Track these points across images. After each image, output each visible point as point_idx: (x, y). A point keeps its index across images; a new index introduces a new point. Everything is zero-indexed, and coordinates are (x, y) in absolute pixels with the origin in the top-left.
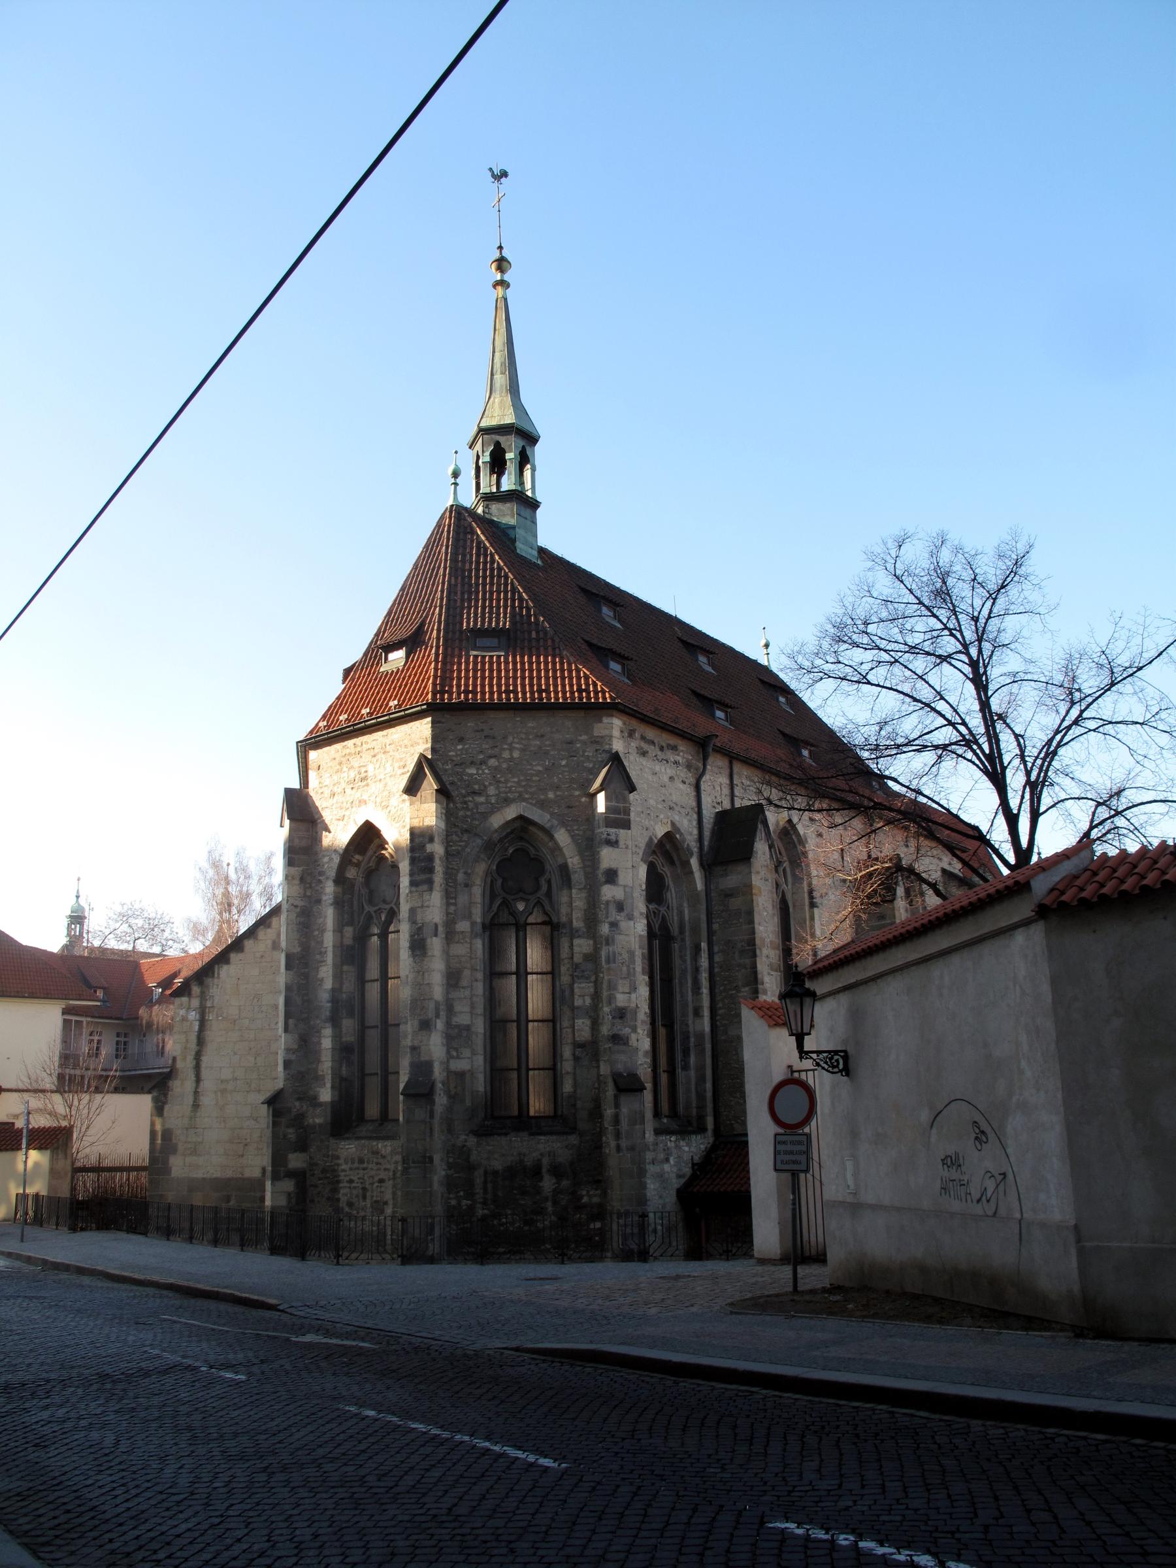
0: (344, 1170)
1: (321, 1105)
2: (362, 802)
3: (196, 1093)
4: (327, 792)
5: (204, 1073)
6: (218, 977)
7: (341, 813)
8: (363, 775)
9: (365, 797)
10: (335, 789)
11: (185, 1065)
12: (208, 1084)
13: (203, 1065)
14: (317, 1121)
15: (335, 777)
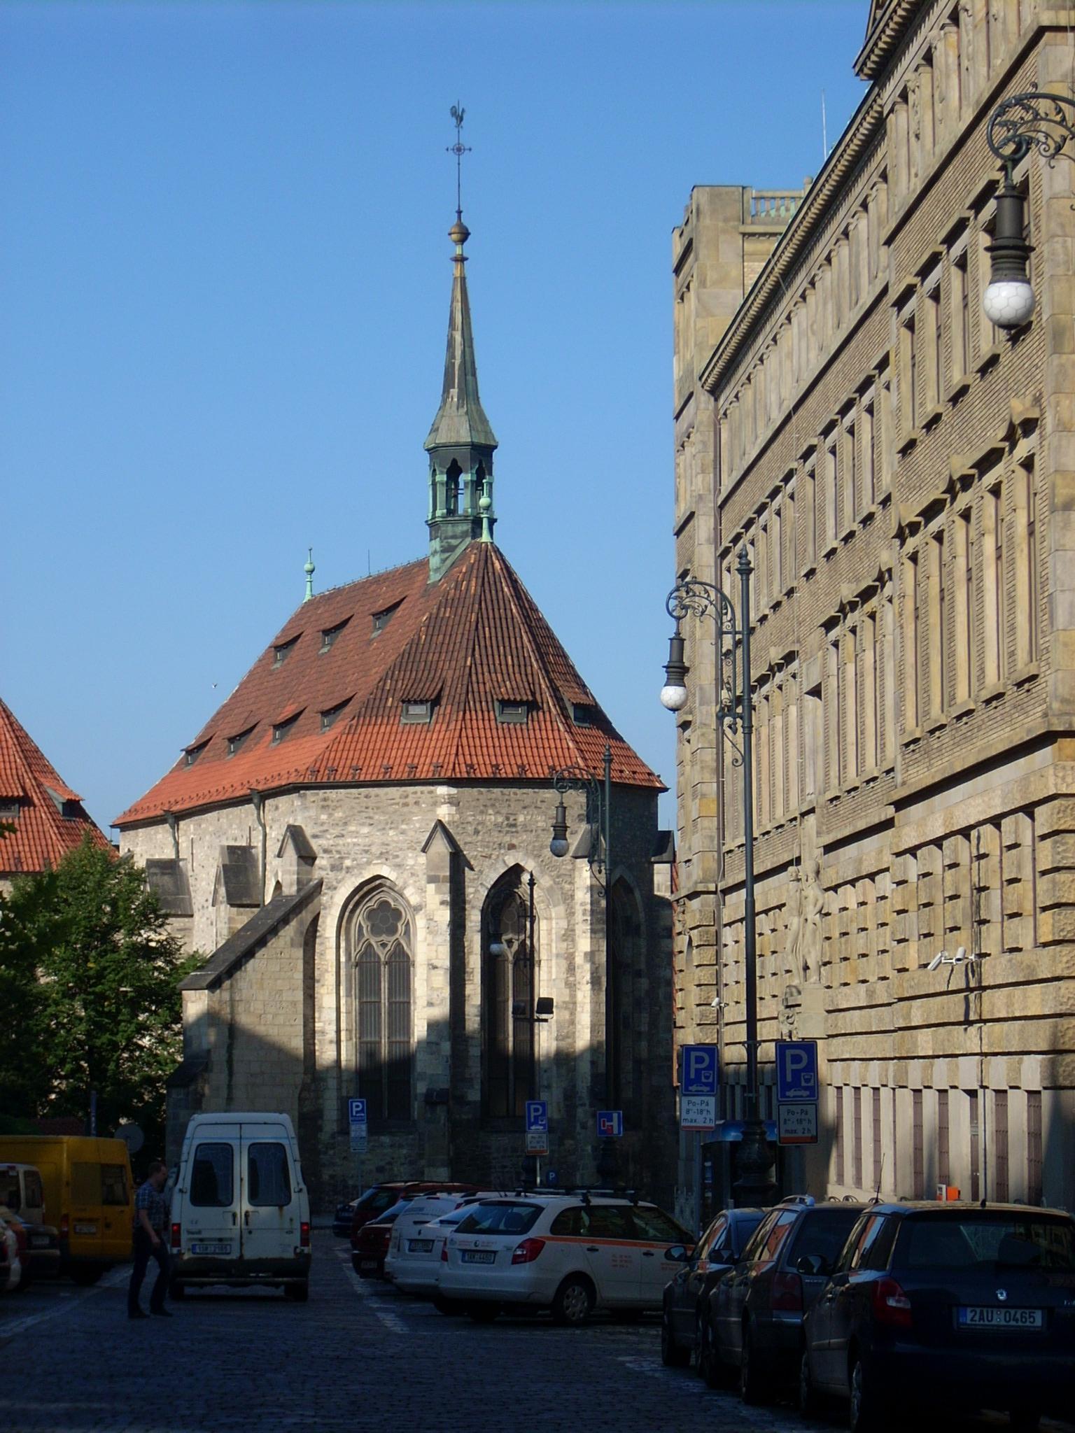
0: (494, 1159)
1: (469, 1103)
2: (512, 847)
3: (230, 1087)
4: (470, 829)
5: (237, 1067)
6: (245, 971)
7: (487, 851)
8: (511, 821)
9: (514, 841)
10: (480, 828)
11: (219, 1057)
12: (239, 1079)
13: (235, 1058)
14: (464, 1117)
15: (479, 818)
